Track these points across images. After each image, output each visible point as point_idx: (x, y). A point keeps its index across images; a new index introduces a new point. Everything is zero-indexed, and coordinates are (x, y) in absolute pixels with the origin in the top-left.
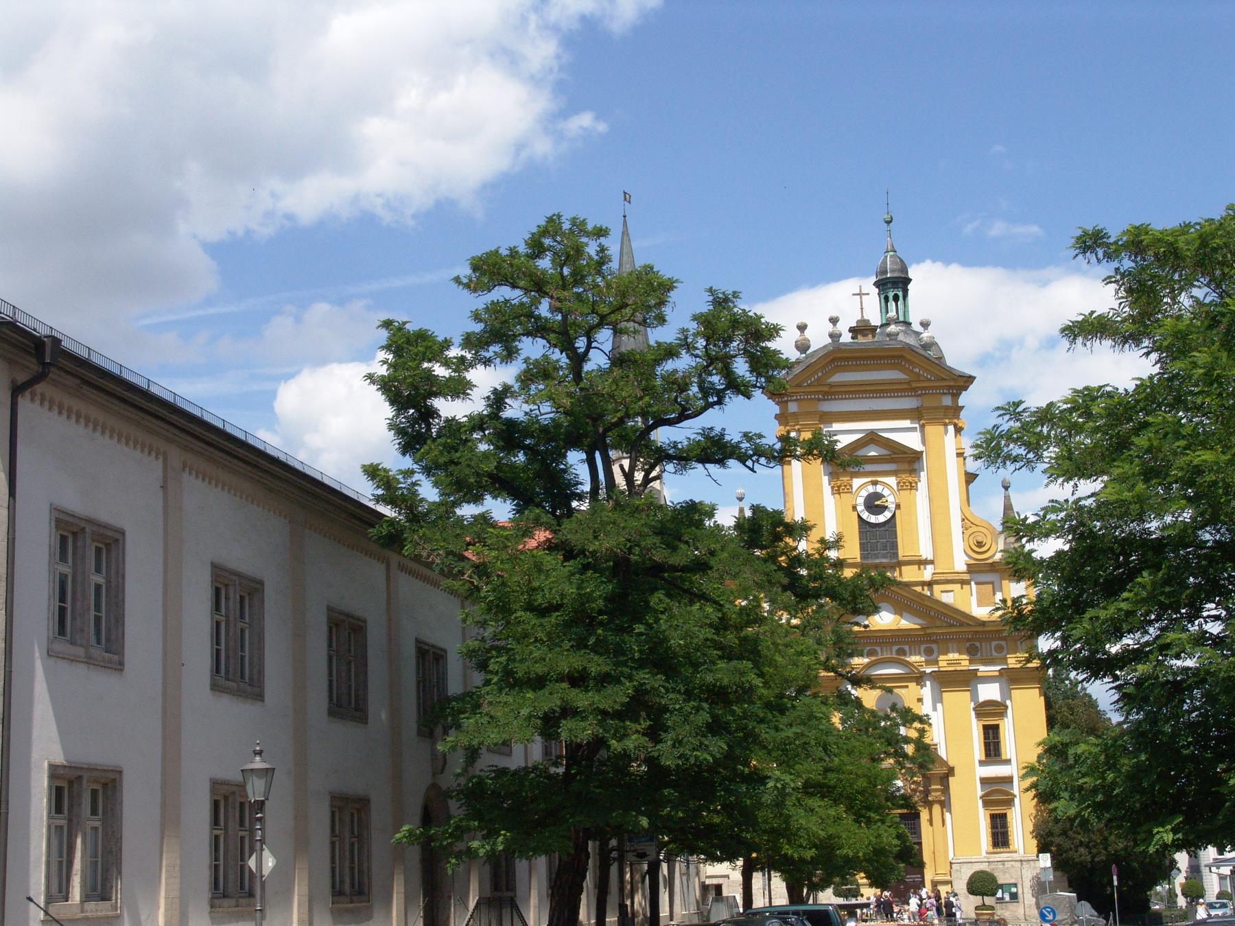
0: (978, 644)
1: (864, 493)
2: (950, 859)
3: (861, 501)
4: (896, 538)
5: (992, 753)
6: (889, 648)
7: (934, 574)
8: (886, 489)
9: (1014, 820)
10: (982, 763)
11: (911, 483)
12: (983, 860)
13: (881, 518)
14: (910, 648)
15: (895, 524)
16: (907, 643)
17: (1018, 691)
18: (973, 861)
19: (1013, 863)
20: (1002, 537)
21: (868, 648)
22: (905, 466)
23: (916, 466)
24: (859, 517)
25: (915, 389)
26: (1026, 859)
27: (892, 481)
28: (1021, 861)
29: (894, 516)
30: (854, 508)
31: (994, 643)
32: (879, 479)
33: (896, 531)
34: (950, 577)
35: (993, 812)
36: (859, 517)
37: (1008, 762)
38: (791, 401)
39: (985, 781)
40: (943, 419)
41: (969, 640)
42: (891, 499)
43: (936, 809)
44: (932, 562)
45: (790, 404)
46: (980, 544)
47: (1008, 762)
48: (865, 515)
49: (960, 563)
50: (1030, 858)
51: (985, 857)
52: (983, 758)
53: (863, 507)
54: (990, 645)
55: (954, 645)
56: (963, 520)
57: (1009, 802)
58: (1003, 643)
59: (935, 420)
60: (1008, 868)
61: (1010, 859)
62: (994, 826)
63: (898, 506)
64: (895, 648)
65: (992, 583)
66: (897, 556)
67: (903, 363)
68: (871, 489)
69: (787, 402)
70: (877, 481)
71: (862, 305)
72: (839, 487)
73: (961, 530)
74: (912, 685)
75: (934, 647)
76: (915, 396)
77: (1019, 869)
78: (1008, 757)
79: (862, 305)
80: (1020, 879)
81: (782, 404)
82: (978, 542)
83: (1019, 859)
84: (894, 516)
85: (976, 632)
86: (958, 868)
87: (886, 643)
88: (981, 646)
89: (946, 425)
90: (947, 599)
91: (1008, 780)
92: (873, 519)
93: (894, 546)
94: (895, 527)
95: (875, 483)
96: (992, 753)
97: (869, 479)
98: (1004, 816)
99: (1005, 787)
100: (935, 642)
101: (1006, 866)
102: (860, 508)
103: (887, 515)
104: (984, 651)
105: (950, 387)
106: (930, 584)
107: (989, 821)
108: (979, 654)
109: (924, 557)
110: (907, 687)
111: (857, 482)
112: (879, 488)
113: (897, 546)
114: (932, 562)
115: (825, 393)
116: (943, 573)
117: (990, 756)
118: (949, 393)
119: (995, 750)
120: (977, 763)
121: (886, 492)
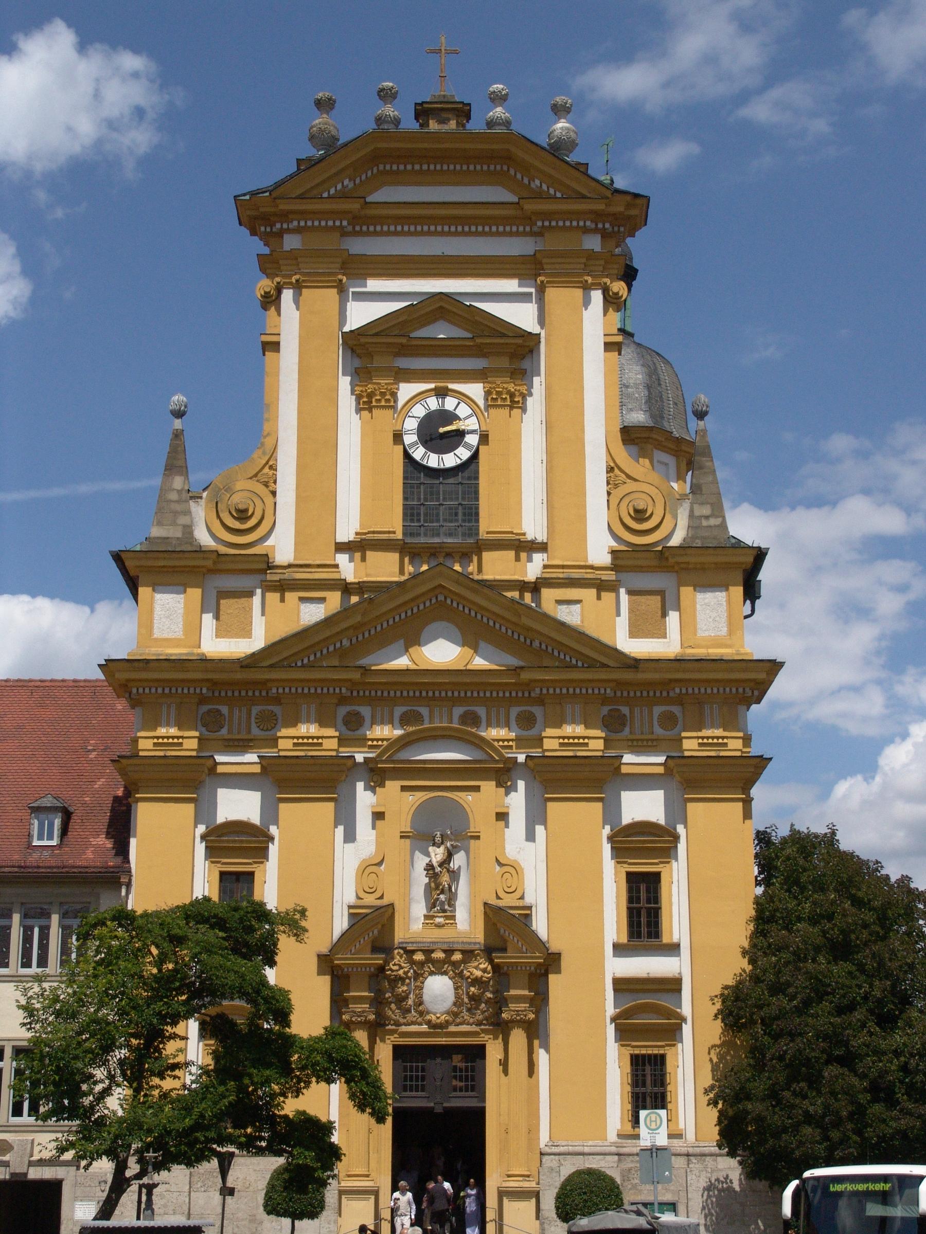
0: (625, 710)
1: (419, 411)
2: (542, 1145)
3: (411, 424)
4: (477, 499)
5: (644, 930)
7: (545, 567)
8: (462, 405)
9: (680, 1070)
11: (512, 395)
12: (607, 1149)
13: (450, 460)
14: (488, 713)
15: (477, 472)
16: (484, 702)
17: (701, 805)
18: (586, 1150)
20: (686, 505)
21: (404, 709)
22: (504, 362)
23: (526, 364)
24: (407, 455)
25: (528, 219)
26: (698, 1150)
27: (475, 390)
28: (688, 1155)
29: (475, 456)
30: (398, 437)
31: (658, 710)
32: (451, 386)
33: (477, 486)
34: (576, 574)
35: (637, 1052)
36: (407, 455)
37: (673, 949)
38: (289, 231)
39: (622, 986)
40: (580, 275)
41: (605, 701)
43: (518, 1038)
44: (542, 547)
45: (286, 237)
46: (640, 515)
47: (673, 949)
48: (418, 453)
50: (706, 1150)
51: (613, 1144)
52: (624, 939)
53: (414, 438)
56: (610, 470)
57: (672, 1033)
58: (676, 710)
59: (566, 278)
63: (484, 438)
64: (458, 711)
65: (661, 593)
66: (478, 534)
67: (512, 172)
68: (433, 403)
69: (280, 234)
70: (447, 389)
72: (370, 395)
73: (604, 488)
74: (488, 786)
75: (537, 711)
76: (532, 234)
77: (683, 1171)
78: (675, 939)
80: (683, 1194)
81: (272, 237)
82: (637, 511)
83: (684, 1150)
84: (475, 456)
85: (619, 684)
86: (554, 1164)
87: (441, 699)
89: (587, 288)
90: (570, 616)
91: (672, 986)
92: (433, 461)
93: (473, 514)
94: (477, 478)
95: (442, 393)
96: (644, 930)
97: (432, 386)
98: (660, 1060)
99: (664, 1001)
100: (540, 701)
102: (410, 439)
103: (463, 454)
104: (637, 725)
105: (598, 216)
106: (535, 587)
107: (628, 1069)
108: (627, 729)
109: (530, 537)
110: (477, 789)
111: (406, 390)
112: (450, 403)
113: (477, 514)
114: (542, 547)
115: (355, 219)
116: (563, 567)
117: (639, 936)
118: (596, 230)
119: (649, 925)
120: (609, 949)
121: (463, 411)
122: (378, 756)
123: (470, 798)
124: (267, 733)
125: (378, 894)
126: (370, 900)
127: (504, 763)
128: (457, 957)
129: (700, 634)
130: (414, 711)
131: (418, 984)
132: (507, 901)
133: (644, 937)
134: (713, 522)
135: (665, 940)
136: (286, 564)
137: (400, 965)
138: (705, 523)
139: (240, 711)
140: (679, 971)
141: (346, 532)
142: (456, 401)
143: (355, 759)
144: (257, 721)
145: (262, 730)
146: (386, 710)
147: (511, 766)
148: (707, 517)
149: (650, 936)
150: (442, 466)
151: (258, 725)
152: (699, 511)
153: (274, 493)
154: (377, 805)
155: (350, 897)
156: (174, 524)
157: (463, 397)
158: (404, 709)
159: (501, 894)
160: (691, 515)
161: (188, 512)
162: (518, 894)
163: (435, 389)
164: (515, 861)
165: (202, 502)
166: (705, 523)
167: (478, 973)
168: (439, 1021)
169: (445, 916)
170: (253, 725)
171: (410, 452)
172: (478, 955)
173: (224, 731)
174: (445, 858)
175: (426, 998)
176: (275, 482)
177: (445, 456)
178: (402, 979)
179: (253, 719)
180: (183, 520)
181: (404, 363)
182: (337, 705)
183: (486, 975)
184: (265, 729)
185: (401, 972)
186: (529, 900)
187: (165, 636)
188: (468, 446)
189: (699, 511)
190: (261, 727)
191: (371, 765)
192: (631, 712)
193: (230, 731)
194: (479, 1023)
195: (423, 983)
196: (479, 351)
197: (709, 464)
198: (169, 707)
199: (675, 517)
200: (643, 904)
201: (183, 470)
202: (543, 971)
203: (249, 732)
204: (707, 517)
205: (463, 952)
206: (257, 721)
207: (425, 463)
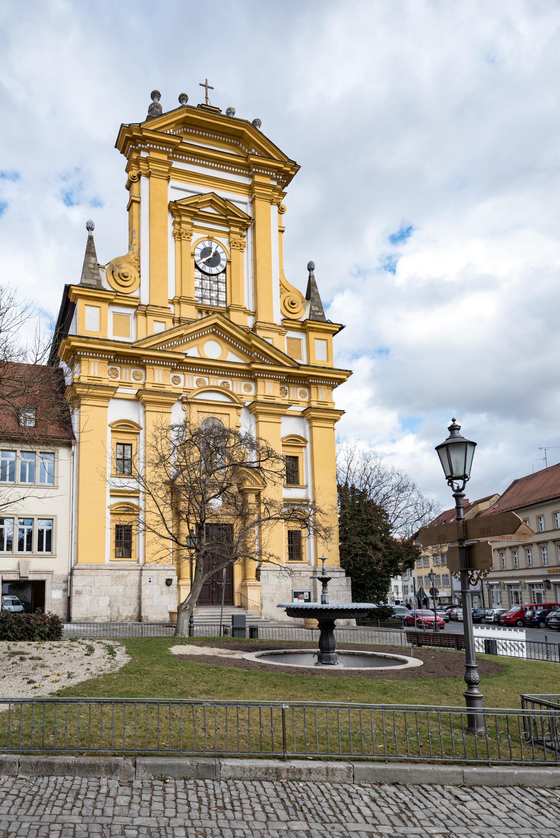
1: (201, 247)
3: (198, 252)
11: (241, 245)
19: (308, 573)
21: (198, 377)
32: (215, 238)
41: (282, 382)
42: (223, 256)
49: (277, 319)
54: (297, 390)
60: (304, 577)
61: (305, 569)
62: (290, 541)
67: (241, 145)
68: (207, 244)
70: (213, 238)
71: (207, 95)
79: (207, 95)
86: (266, 574)
97: (207, 236)
101: (302, 575)
108: (287, 396)
116: (264, 323)
129: (316, 359)
134: (320, 314)
136: (147, 304)
138: (317, 314)
141: (171, 296)
142: (217, 245)
148: (317, 312)
150: (211, 273)
152: (314, 308)
153: (139, 272)
156: (93, 279)
157: (220, 244)
160: (311, 310)
161: (98, 275)
163: (208, 237)
165: (105, 271)
166: (317, 314)
170: (132, 377)
171: (198, 264)
176: (139, 267)
177: (212, 268)
180: (96, 277)
181: (196, 223)
187: (91, 330)
188: (222, 266)
189: (314, 308)
196: (227, 223)
197: (316, 290)
198: (94, 364)
199: (305, 309)
201: (94, 255)
204: (317, 312)
207: (204, 270)
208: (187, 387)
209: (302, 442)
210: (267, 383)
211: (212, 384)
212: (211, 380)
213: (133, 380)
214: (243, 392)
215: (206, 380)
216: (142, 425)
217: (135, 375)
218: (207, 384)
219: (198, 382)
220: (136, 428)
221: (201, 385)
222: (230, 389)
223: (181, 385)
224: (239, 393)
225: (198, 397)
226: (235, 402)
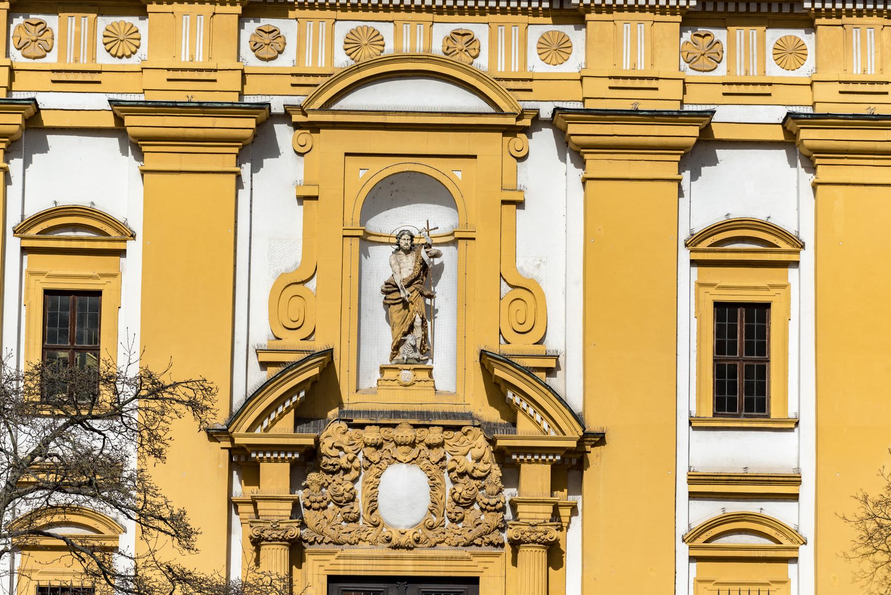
5: (741, 397)
6: (420, 29)
10: (696, 424)
52: (708, 410)
54: (762, 41)
55: (641, 29)
88: (731, 40)
96: (741, 397)
104: (739, 56)
117: (732, 407)
119: (749, 388)
122: (310, 101)
123: (459, 175)
124: (124, 61)
125: (305, 332)
126: (292, 340)
127: (518, 119)
128: (434, 435)
130: (368, 28)
131: (371, 478)
132: (519, 345)
133: (741, 410)
135: (775, 411)
137: (340, 449)
139: (78, 24)
140: (796, 466)
143: (270, 109)
144: (107, 40)
145: (114, 56)
146: (323, 27)
147: (526, 122)
149: (749, 408)
151: (108, 47)
154: (306, 185)
155: (261, 334)
158: (354, 25)
159: (508, 334)
162: (536, 336)
164: (533, 281)
167: (468, 463)
168: (403, 540)
169: (415, 369)
170: (101, 48)
172: (466, 434)
173: (52, 60)
174: (416, 274)
175: (382, 501)
178: (347, 471)
179: (100, 40)
182: (242, 19)
183: (481, 466)
184: (120, 54)
185: (343, 462)
186: (553, 343)
190: (113, 51)
191: (297, 118)
192: (731, 40)
193: (62, 56)
194: (470, 544)
195: (378, 477)
200: (741, 355)
202: (574, 462)
203: (94, 59)
205: (446, 428)
206: (107, 40)
208: (308, 65)
209: (783, 246)
210: (626, 30)
211: (406, 47)
212: (406, 29)
213: (104, 59)
214: (537, 65)
215: (386, 31)
216: (136, 224)
217: (112, 41)
218: (390, 48)
219: (352, 44)
220: (114, 234)
221: (367, 53)
222: (482, 62)
223: (285, 62)
224: (515, 70)
225: (352, 101)
226: (500, 112)
